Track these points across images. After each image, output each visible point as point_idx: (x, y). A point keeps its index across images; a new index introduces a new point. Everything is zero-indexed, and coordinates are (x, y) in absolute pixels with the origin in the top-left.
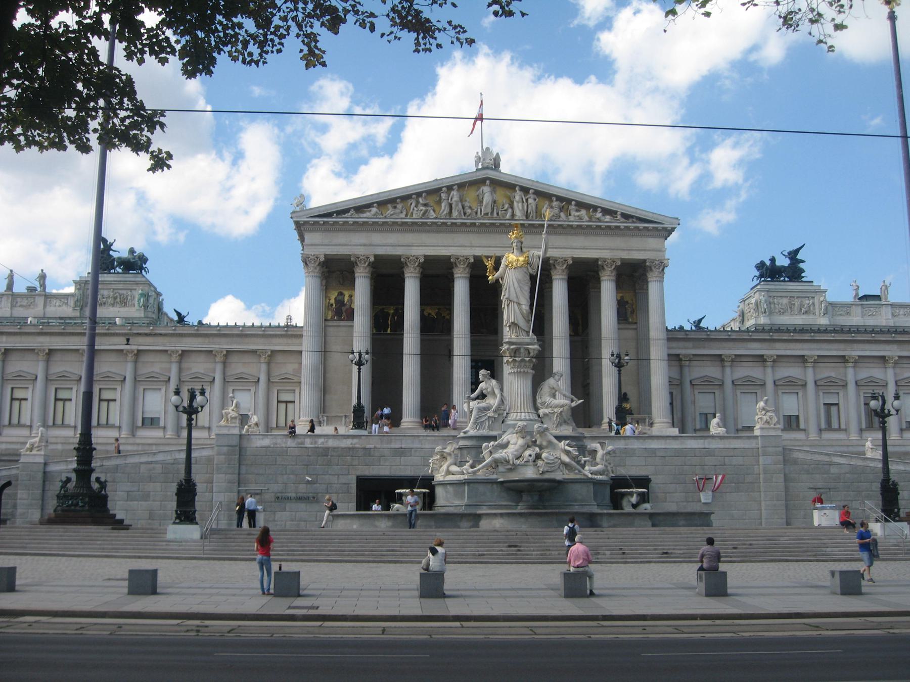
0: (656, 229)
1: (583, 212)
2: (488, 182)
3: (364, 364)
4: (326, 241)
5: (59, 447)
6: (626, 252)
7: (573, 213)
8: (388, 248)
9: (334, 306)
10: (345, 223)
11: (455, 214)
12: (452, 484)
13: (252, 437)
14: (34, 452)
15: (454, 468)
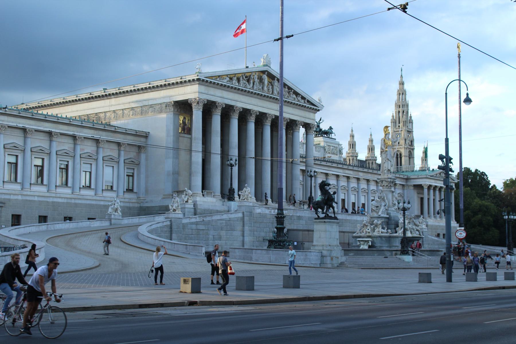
0: (316, 109)
1: (294, 96)
2: (267, 73)
3: (233, 166)
4: (206, 92)
5: (20, 197)
6: (304, 118)
7: (291, 95)
8: (229, 100)
9: (182, 125)
10: (218, 84)
11: (255, 87)
12: (385, 237)
13: (255, 208)
14: (177, 212)
15: (383, 230)
